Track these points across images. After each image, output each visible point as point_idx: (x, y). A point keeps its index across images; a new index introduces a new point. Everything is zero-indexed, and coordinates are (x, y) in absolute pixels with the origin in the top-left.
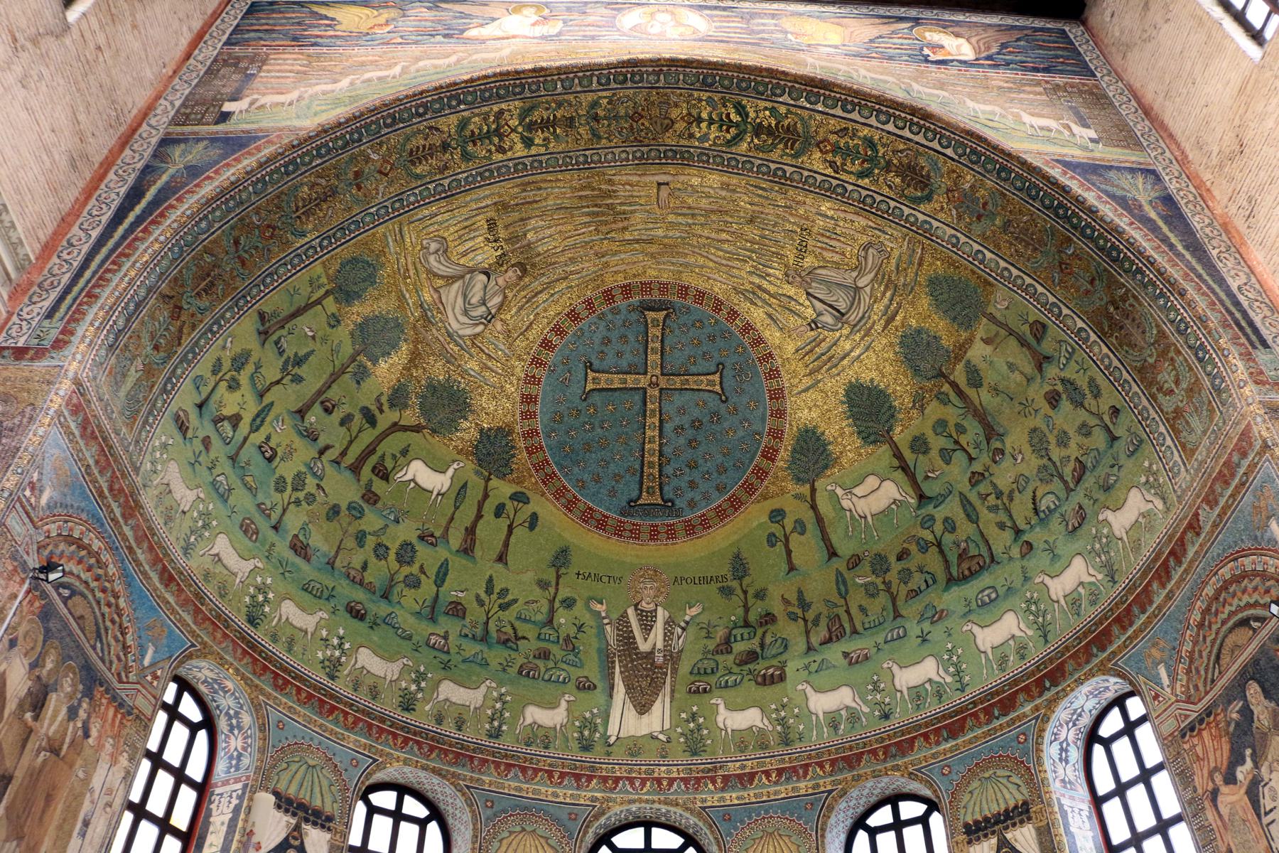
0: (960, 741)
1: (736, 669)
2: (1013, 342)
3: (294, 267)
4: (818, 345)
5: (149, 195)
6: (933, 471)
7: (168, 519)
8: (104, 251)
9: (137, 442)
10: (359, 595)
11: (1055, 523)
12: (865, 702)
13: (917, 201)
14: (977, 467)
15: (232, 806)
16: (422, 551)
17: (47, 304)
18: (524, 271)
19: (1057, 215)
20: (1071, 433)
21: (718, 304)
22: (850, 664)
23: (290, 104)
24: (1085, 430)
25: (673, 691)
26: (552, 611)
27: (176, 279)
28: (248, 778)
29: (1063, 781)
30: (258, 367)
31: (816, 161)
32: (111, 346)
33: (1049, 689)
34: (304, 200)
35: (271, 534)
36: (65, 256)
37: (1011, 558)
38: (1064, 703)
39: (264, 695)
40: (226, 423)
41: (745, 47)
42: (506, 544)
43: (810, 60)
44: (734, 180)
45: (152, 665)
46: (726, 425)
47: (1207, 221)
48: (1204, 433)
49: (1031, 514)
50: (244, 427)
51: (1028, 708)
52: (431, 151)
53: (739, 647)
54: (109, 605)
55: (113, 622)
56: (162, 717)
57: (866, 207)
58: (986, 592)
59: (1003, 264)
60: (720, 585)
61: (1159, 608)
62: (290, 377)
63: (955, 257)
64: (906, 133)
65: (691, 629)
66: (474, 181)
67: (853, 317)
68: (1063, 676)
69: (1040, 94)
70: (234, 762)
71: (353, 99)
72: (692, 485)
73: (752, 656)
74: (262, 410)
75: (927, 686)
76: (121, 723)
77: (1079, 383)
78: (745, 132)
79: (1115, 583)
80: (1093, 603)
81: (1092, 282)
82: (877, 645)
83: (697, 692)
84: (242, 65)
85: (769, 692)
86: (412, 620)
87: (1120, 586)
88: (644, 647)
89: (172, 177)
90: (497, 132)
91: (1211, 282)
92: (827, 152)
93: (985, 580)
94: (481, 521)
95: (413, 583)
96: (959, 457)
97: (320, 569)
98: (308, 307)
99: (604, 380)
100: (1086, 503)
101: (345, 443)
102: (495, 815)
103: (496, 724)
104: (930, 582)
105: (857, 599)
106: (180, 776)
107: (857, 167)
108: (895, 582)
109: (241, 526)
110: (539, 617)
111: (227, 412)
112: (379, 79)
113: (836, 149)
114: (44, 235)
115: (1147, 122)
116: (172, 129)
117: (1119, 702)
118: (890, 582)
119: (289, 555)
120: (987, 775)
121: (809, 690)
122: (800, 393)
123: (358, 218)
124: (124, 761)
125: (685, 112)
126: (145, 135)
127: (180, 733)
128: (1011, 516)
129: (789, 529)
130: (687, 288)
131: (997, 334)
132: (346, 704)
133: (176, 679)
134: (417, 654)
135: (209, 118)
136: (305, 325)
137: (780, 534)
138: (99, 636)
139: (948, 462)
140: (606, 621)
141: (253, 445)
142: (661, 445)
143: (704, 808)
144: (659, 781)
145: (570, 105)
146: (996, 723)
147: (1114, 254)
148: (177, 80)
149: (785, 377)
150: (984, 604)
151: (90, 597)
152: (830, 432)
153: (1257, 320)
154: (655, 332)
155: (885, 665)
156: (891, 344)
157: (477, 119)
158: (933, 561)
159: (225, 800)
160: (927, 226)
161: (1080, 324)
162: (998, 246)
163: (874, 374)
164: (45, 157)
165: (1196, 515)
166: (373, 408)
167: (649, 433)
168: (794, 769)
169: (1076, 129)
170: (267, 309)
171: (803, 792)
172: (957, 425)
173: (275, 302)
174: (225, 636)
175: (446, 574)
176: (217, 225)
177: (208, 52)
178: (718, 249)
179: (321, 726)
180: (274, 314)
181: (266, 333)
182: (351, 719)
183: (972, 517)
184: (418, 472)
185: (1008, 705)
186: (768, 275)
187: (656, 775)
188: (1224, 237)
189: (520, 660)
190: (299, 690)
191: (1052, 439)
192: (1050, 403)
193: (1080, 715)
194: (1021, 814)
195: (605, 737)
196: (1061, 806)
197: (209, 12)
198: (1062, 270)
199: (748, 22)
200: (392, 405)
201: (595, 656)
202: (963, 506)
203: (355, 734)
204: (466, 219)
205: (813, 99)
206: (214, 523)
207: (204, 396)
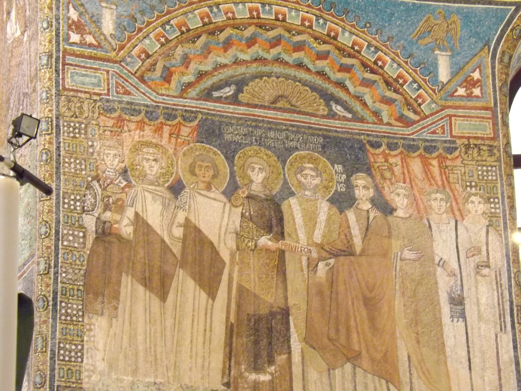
54: (322, 56)
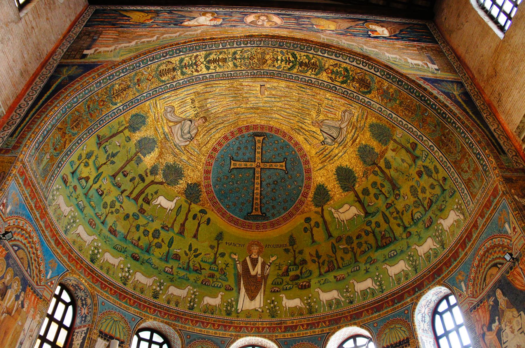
0: (381, 313)
1: (290, 283)
2: (403, 151)
3: (112, 117)
4: (325, 151)
5: (53, 88)
6: (371, 203)
7: (59, 219)
8: (34, 110)
9: (47, 187)
10: (137, 251)
11: (420, 224)
12: (343, 296)
13: (366, 93)
14: (389, 201)
15: (82, 337)
16: (163, 233)
17: (10, 131)
18: (206, 120)
19: (421, 100)
20: (427, 188)
21: (285, 134)
22: (337, 281)
23: (111, 51)
24: (432, 187)
25: (264, 291)
26: (215, 258)
27: (64, 121)
28: (89, 325)
29: (423, 330)
30: (97, 157)
31: (324, 76)
32: (37, 148)
33: (417, 292)
34: (116, 90)
35: (101, 226)
36: (18, 111)
37: (402, 238)
38: (423, 298)
39: (97, 291)
40: (83, 180)
41: (296, 31)
42: (197, 230)
43: (322, 36)
44: (291, 84)
45: (50, 278)
46: (287, 183)
47: (482, 103)
48: (480, 188)
49: (411, 221)
50: (91, 182)
51: (409, 300)
52: (168, 71)
53: (291, 273)
54: (34, 253)
55: (35, 260)
56: (54, 300)
57: (345, 95)
58: (392, 252)
59: (399, 119)
60: (284, 248)
61: (462, 259)
62: (109, 162)
63: (380, 116)
64: (361, 66)
65: (272, 266)
66: (186, 83)
67: (339, 140)
68: (423, 286)
69: (415, 50)
70: (83, 319)
71: (137, 50)
72: (273, 207)
73: (297, 277)
74: (98, 175)
75: (368, 290)
76: (37, 302)
77: (430, 168)
78: (296, 65)
79: (444, 249)
80: (435, 257)
81: (435, 127)
82: (348, 273)
83: (274, 291)
84: (92, 35)
85: (304, 292)
86: (158, 261)
87: (446, 250)
88: (253, 273)
89: (62, 80)
90: (195, 64)
91: (483, 127)
92: (329, 73)
93: (392, 247)
94: (187, 221)
95: (159, 246)
96: (381, 197)
97: (120, 240)
98: (118, 133)
99: (238, 164)
100: (433, 216)
101: (132, 189)
102: (191, 341)
103: (192, 304)
104: (370, 248)
105: (340, 254)
106: (61, 324)
107: (341, 79)
108: (356, 247)
109: (89, 222)
110: (210, 260)
111: (84, 175)
112: (148, 41)
113: (332, 72)
114: (10, 103)
115: (459, 62)
116: (62, 60)
117: (446, 297)
118: (353, 248)
119: (108, 234)
120: (392, 327)
121: (320, 291)
122: (317, 170)
123: (139, 98)
124: (38, 317)
125: (272, 57)
126: (51, 63)
127: (61, 307)
128: (402, 221)
129: (313, 225)
130: (272, 127)
131: (397, 147)
132: (130, 295)
133: (60, 284)
134: (160, 275)
135: (78, 56)
136: (116, 140)
137: (309, 227)
138: (29, 266)
139: (377, 199)
140: (237, 262)
141: (94, 189)
142: (261, 191)
143: (276, 339)
144: (258, 328)
145: (225, 53)
146: (396, 306)
147: (444, 115)
148: (65, 41)
149: (312, 164)
150: (391, 257)
151: (26, 250)
152: (329, 187)
153: (501, 143)
154: (259, 145)
155: (351, 282)
156: (354, 151)
157: (187, 58)
158: (371, 239)
159: (79, 335)
160: (369, 104)
161: (431, 144)
162: (397, 112)
163: (347, 163)
164: (10, 72)
165: (476, 221)
166: (144, 175)
167: (256, 186)
168: (314, 324)
169: (430, 65)
170: (101, 134)
171: (317, 333)
172: (381, 184)
173: (104, 131)
174: (81, 267)
175: (172, 242)
176: (81, 100)
177: (78, 30)
178: (285, 112)
179: (120, 304)
180: (104, 136)
181: (100, 144)
182: (132, 302)
183: (387, 221)
184: (162, 201)
185: (401, 298)
186: (305, 123)
187: (257, 326)
188: (489, 109)
189: (202, 278)
190: (111, 289)
191: (419, 190)
192: (418, 175)
193: (430, 303)
194: (405, 343)
195: (237, 310)
196: (422, 340)
197: (78, 13)
198: (423, 122)
199: (297, 20)
200: (151, 174)
201: (233, 277)
202: (383, 217)
203: (134, 307)
204: (182, 99)
205: (323, 52)
206: (78, 221)
207: (74, 169)
